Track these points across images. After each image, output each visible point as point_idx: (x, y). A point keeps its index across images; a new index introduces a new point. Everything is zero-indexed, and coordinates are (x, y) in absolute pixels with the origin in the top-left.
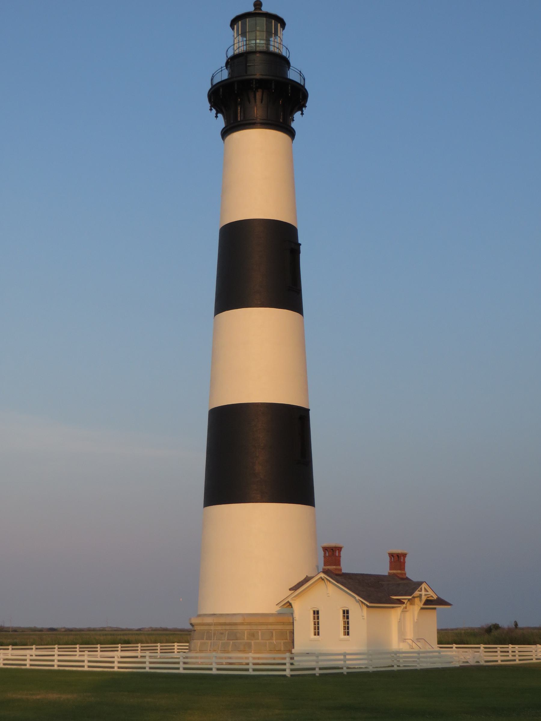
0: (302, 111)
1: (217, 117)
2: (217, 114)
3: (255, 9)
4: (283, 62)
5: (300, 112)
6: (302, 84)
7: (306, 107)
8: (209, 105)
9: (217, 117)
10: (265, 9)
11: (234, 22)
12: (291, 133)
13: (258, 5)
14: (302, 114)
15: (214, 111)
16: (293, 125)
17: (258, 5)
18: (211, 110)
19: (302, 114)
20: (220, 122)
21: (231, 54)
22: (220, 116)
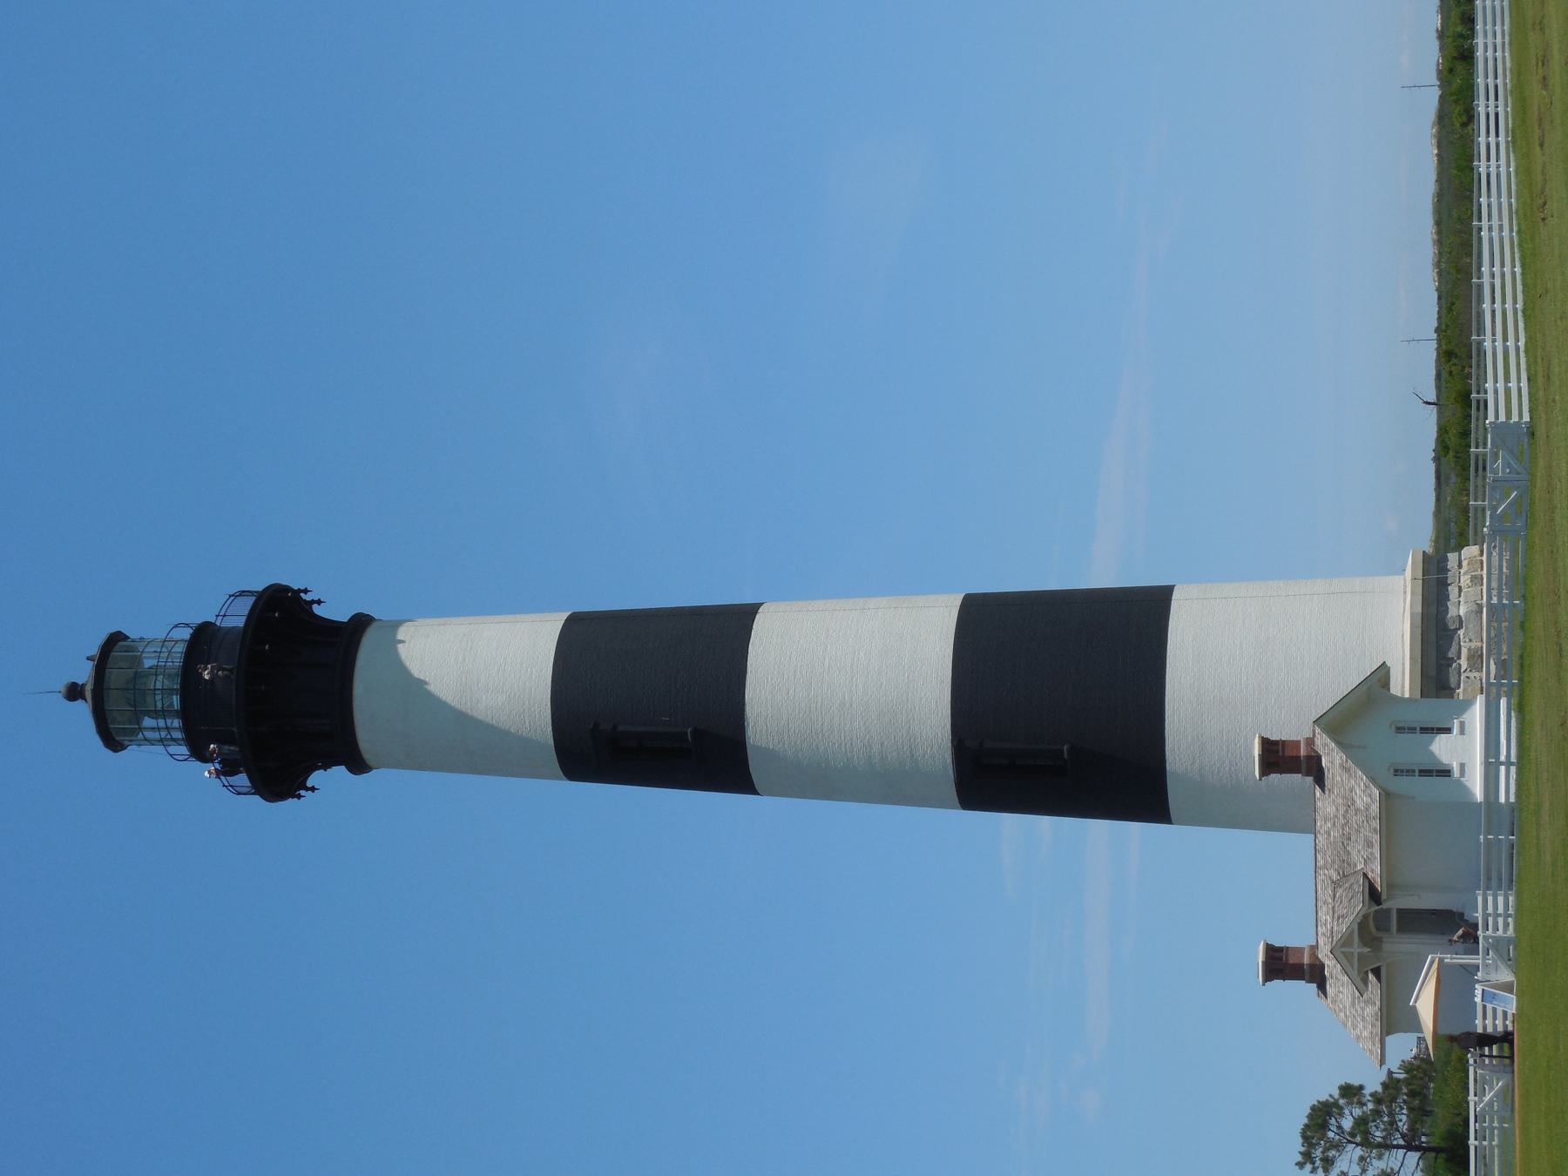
0: (313, 602)
1: (313, 789)
2: (307, 789)
3: (84, 698)
4: (203, 638)
5: (316, 609)
7: (306, 591)
8: (291, 802)
9: (313, 789)
10: (83, 674)
11: (112, 741)
12: (361, 623)
13: (74, 692)
14: (319, 602)
15: (302, 792)
16: (343, 617)
17: (74, 692)
18: (299, 797)
19: (319, 602)
20: (330, 781)
21: (183, 750)
22: (315, 778)
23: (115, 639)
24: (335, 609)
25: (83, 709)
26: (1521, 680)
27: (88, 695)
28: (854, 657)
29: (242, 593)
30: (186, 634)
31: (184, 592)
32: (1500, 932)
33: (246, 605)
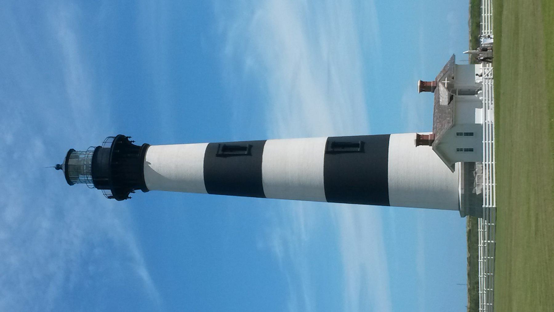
6: (113, 139)
7: (130, 137)
10: (62, 162)
11: (70, 182)
13: (58, 167)
17: (58, 167)
21: (92, 185)
23: (71, 151)
24: (138, 143)
25: (61, 172)
26: (493, 304)
27: (64, 167)
28: (294, 153)
29: (109, 137)
30: (93, 149)
31: (91, 137)
32: (491, 206)
33: (112, 140)
